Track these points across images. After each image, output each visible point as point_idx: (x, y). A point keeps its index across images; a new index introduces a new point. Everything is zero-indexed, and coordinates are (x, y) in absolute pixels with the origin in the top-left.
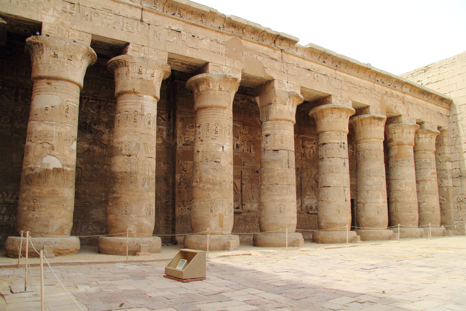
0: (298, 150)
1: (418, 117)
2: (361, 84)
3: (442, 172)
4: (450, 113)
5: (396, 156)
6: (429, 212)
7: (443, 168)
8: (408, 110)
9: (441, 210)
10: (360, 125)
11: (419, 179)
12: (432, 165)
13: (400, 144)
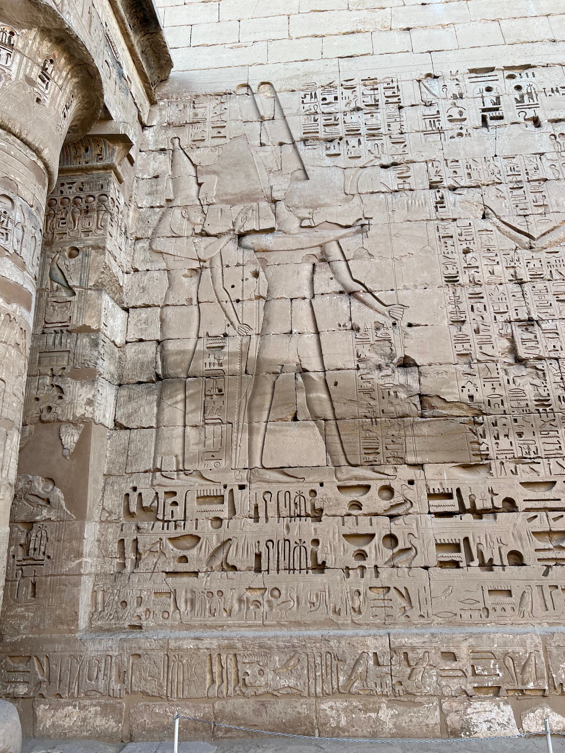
3: (68, 342)
7: (77, 322)
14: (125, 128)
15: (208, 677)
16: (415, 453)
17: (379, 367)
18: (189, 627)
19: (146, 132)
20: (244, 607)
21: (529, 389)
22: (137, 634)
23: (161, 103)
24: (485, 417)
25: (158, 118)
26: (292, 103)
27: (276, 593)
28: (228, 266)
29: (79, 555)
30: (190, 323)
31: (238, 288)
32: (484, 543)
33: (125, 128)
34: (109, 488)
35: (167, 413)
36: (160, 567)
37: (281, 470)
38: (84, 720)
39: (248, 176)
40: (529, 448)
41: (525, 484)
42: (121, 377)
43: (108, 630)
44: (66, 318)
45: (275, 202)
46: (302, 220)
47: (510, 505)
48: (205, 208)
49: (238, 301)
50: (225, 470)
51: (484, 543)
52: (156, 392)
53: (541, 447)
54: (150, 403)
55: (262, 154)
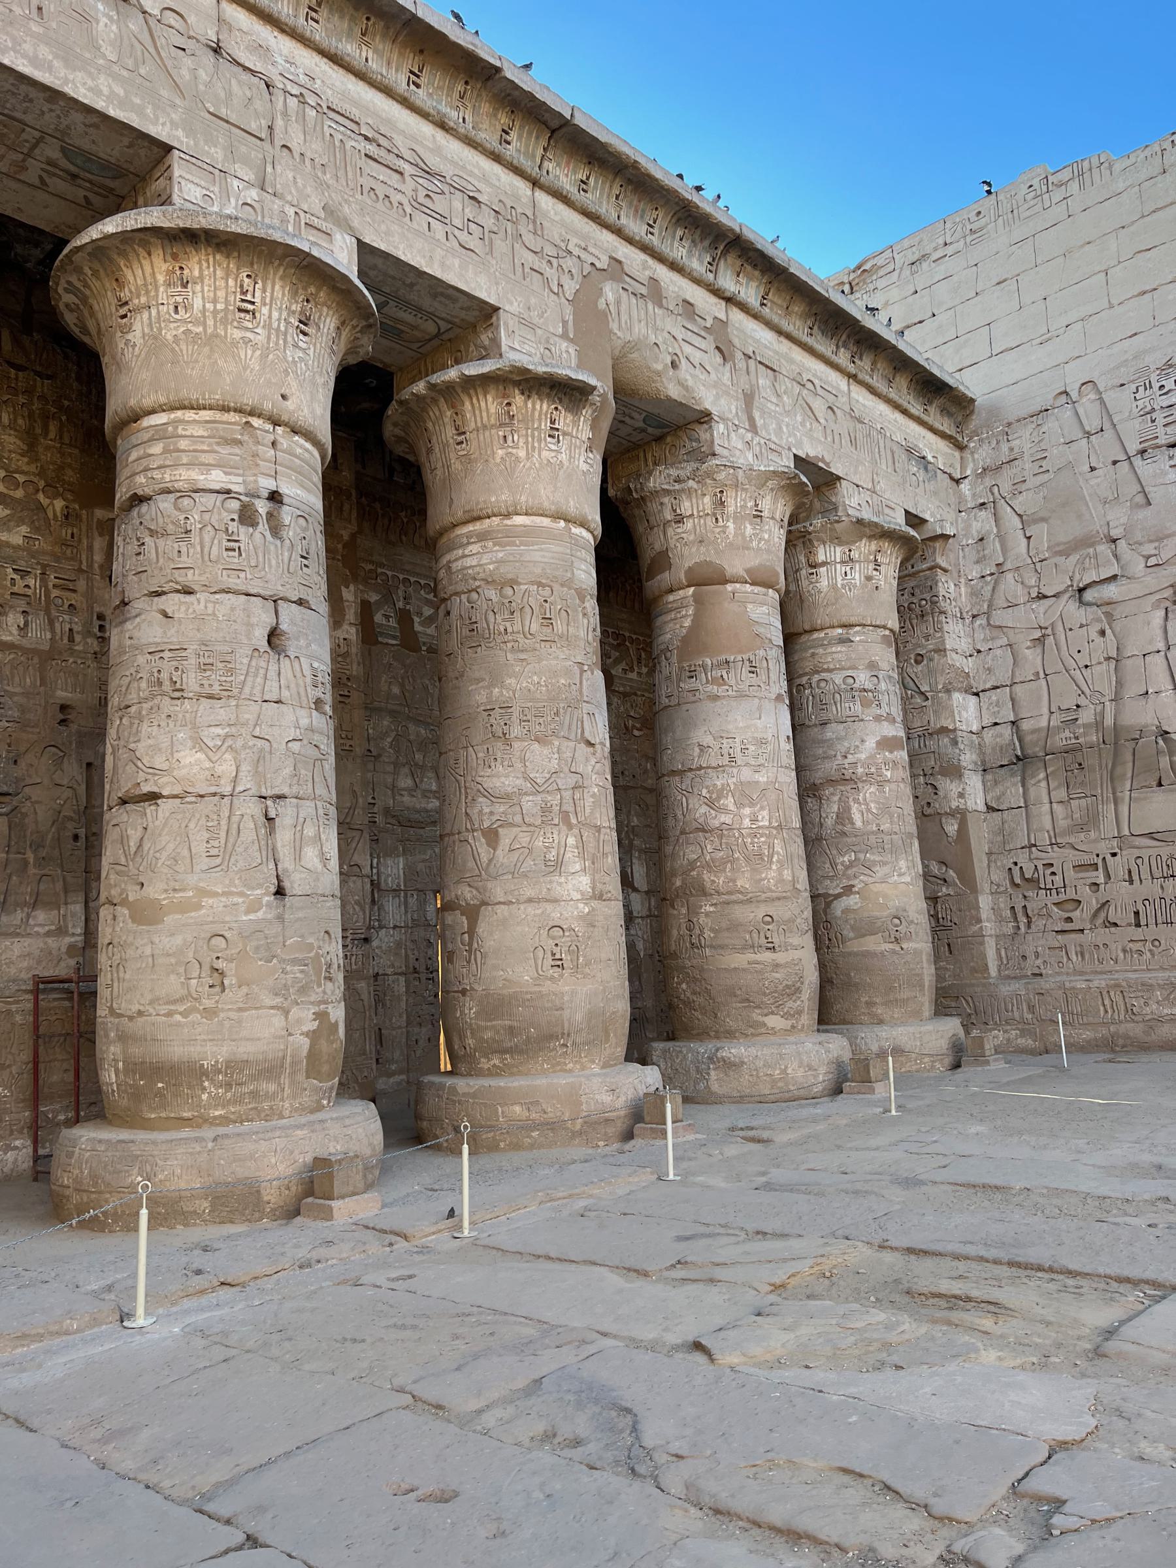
0: (74, 599)
1: (809, 450)
2: (433, 162)
4: (963, 467)
5: (693, 643)
6: (875, 944)
7: (936, 724)
8: (749, 399)
9: (934, 932)
10: (450, 431)
11: (818, 777)
12: (884, 699)
13: (708, 578)
14: (942, 527)
15: (1102, 1008)
18: (1082, 973)
19: (962, 486)
20: (1128, 956)
22: (1038, 979)
23: (972, 445)
25: (971, 465)
26: (1122, 402)
27: (1157, 943)
28: (1071, 630)
29: (979, 921)
30: (1040, 698)
31: (1085, 652)
33: (942, 527)
34: (993, 865)
35: (1032, 792)
36: (1049, 927)
37: (1150, 835)
38: (1008, 1040)
39: (1080, 516)
42: (983, 762)
43: (1015, 978)
44: (926, 723)
45: (1114, 541)
46: (1148, 557)
48: (1038, 565)
49: (1086, 667)
50: (1095, 841)
52: (1019, 773)
54: (1015, 785)
55: (1093, 482)
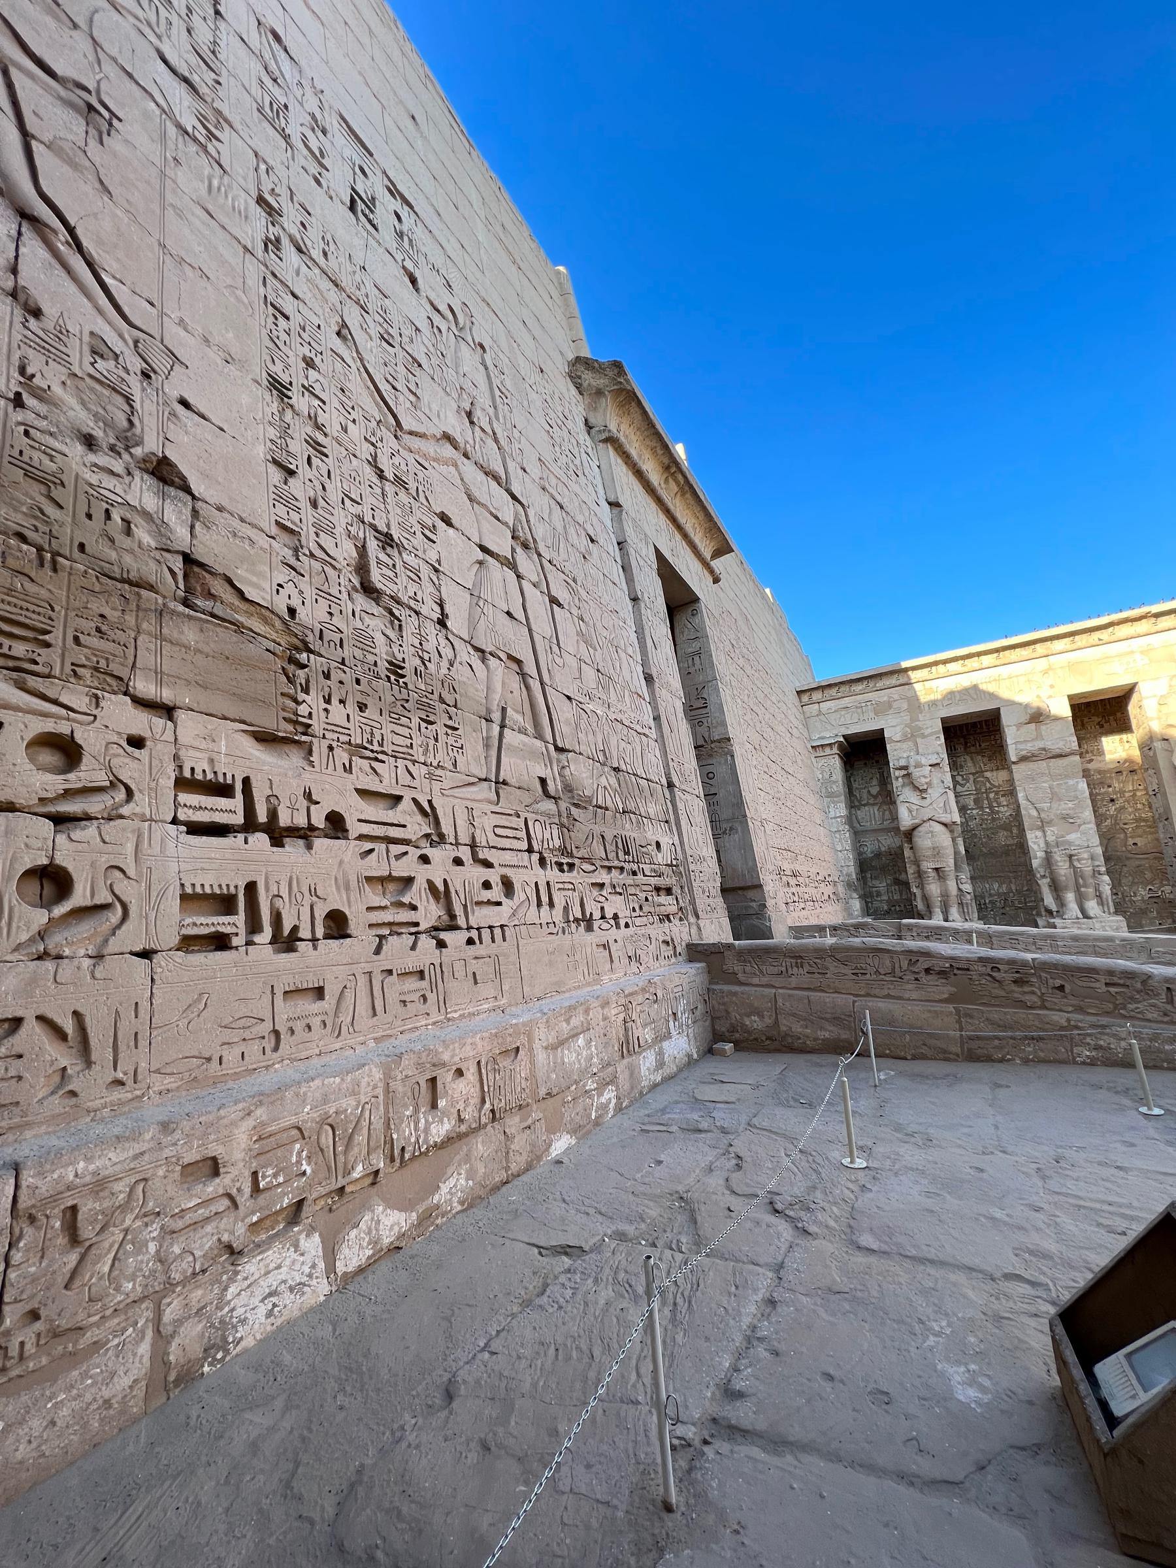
16: (160, 676)
17: (89, 442)
21: (380, 640)
24: (312, 656)
32: (284, 893)
40: (372, 734)
41: (363, 793)
47: (336, 824)
51: (284, 893)
53: (389, 737)
